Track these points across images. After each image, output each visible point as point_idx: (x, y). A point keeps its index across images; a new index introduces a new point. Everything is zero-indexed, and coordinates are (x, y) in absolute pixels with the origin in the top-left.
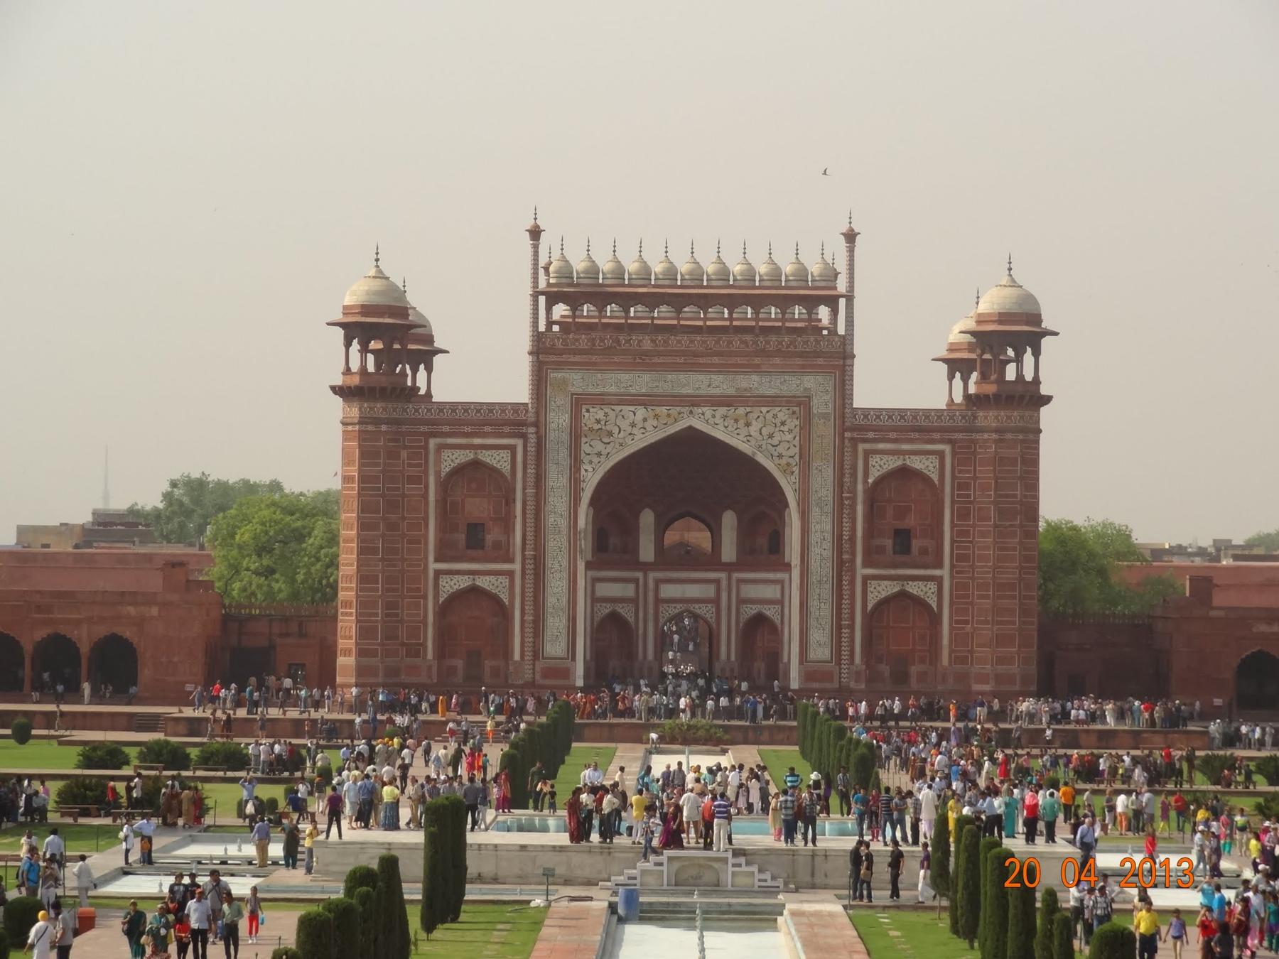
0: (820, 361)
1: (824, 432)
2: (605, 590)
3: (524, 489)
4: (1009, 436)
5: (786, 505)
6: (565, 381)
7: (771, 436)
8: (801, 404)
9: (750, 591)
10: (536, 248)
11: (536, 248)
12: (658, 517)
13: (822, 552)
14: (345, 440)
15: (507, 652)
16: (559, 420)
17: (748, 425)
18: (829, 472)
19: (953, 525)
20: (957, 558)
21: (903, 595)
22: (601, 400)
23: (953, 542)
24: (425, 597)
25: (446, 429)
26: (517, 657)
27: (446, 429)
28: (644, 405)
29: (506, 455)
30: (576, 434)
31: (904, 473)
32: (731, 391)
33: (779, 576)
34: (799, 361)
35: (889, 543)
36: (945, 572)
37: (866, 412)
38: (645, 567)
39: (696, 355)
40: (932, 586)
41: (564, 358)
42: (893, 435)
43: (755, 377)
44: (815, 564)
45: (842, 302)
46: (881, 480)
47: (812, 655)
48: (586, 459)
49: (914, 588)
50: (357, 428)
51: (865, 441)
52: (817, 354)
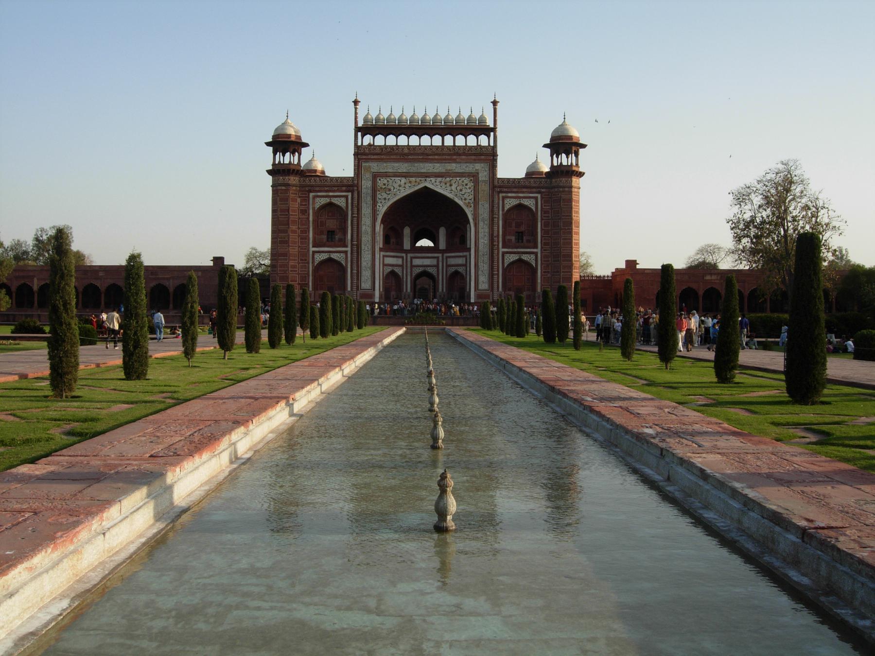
0: (483, 157)
1: (484, 188)
2: (389, 261)
3: (352, 214)
4: (567, 189)
5: (468, 222)
6: (370, 167)
7: (461, 190)
8: (474, 176)
9: (452, 261)
10: (356, 109)
11: (356, 109)
12: (412, 231)
13: (484, 241)
14: (273, 194)
15: (344, 288)
16: (366, 184)
17: (451, 185)
18: (487, 206)
19: (542, 229)
20: (544, 244)
21: (520, 261)
22: (386, 175)
23: (542, 237)
24: (308, 263)
25: (318, 189)
26: (349, 289)
27: (318, 189)
28: (405, 177)
29: (343, 200)
30: (374, 190)
31: (520, 207)
32: (444, 171)
33: (465, 254)
34: (473, 157)
35: (513, 238)
36: (539, 250)
37: (503, 180)
38: (407, 252)
39: (427, 155)
40: (533, 256)
41: (369, 157)
42: (515, 190)
43: (454, 165)
44: (481, 248)
45: (492, 134)
46: (509, 210)
47: (480, 288)
48: (379, 201)
49: (525, 257)
50: (279, 188)
51: (501, 192)
52: (481, 155)
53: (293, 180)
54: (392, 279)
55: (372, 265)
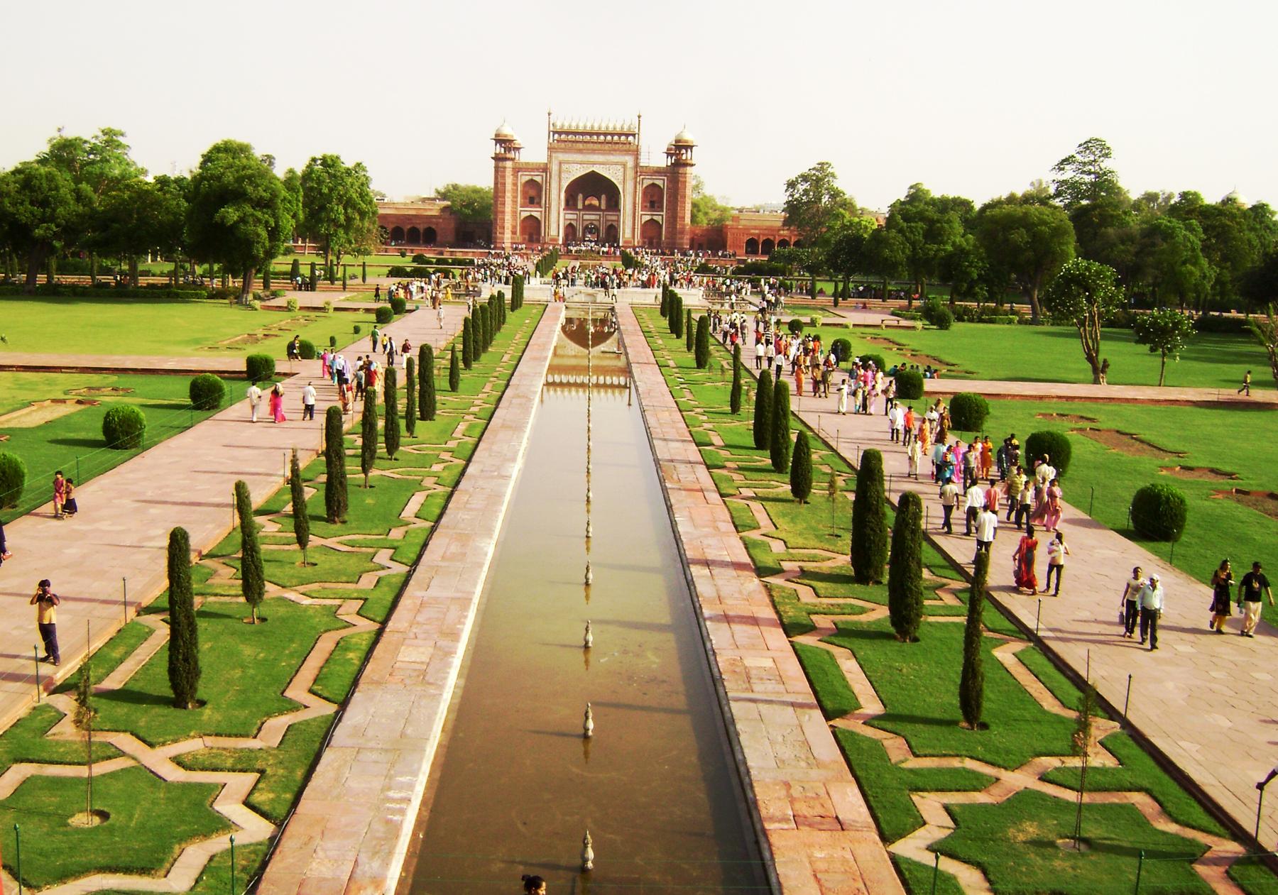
1: (630, 174)
8: (624, 165)
9: (609, 218)
16: (555, 168)
22: (568, 162)
31: (653, 185)
53: (509, 164)
54: (570, 228)
55: (557, 221)
